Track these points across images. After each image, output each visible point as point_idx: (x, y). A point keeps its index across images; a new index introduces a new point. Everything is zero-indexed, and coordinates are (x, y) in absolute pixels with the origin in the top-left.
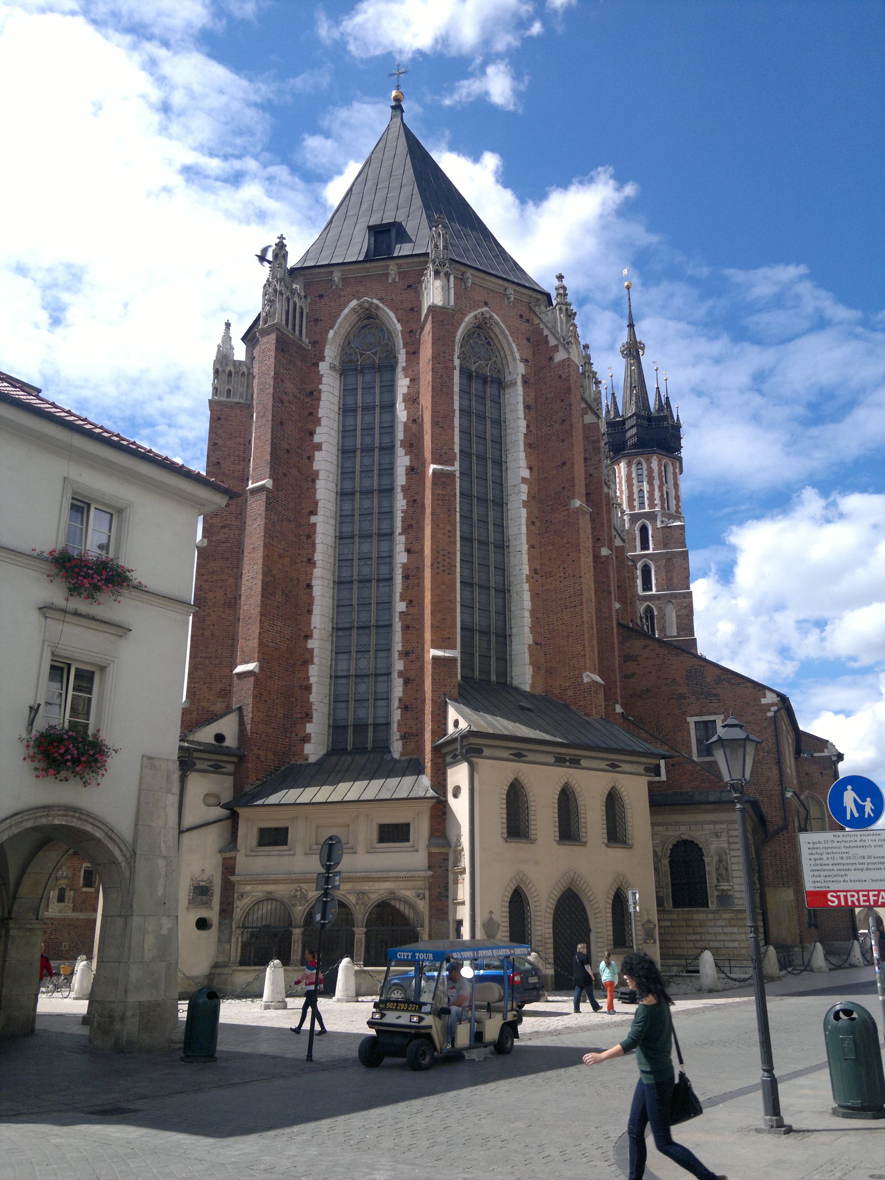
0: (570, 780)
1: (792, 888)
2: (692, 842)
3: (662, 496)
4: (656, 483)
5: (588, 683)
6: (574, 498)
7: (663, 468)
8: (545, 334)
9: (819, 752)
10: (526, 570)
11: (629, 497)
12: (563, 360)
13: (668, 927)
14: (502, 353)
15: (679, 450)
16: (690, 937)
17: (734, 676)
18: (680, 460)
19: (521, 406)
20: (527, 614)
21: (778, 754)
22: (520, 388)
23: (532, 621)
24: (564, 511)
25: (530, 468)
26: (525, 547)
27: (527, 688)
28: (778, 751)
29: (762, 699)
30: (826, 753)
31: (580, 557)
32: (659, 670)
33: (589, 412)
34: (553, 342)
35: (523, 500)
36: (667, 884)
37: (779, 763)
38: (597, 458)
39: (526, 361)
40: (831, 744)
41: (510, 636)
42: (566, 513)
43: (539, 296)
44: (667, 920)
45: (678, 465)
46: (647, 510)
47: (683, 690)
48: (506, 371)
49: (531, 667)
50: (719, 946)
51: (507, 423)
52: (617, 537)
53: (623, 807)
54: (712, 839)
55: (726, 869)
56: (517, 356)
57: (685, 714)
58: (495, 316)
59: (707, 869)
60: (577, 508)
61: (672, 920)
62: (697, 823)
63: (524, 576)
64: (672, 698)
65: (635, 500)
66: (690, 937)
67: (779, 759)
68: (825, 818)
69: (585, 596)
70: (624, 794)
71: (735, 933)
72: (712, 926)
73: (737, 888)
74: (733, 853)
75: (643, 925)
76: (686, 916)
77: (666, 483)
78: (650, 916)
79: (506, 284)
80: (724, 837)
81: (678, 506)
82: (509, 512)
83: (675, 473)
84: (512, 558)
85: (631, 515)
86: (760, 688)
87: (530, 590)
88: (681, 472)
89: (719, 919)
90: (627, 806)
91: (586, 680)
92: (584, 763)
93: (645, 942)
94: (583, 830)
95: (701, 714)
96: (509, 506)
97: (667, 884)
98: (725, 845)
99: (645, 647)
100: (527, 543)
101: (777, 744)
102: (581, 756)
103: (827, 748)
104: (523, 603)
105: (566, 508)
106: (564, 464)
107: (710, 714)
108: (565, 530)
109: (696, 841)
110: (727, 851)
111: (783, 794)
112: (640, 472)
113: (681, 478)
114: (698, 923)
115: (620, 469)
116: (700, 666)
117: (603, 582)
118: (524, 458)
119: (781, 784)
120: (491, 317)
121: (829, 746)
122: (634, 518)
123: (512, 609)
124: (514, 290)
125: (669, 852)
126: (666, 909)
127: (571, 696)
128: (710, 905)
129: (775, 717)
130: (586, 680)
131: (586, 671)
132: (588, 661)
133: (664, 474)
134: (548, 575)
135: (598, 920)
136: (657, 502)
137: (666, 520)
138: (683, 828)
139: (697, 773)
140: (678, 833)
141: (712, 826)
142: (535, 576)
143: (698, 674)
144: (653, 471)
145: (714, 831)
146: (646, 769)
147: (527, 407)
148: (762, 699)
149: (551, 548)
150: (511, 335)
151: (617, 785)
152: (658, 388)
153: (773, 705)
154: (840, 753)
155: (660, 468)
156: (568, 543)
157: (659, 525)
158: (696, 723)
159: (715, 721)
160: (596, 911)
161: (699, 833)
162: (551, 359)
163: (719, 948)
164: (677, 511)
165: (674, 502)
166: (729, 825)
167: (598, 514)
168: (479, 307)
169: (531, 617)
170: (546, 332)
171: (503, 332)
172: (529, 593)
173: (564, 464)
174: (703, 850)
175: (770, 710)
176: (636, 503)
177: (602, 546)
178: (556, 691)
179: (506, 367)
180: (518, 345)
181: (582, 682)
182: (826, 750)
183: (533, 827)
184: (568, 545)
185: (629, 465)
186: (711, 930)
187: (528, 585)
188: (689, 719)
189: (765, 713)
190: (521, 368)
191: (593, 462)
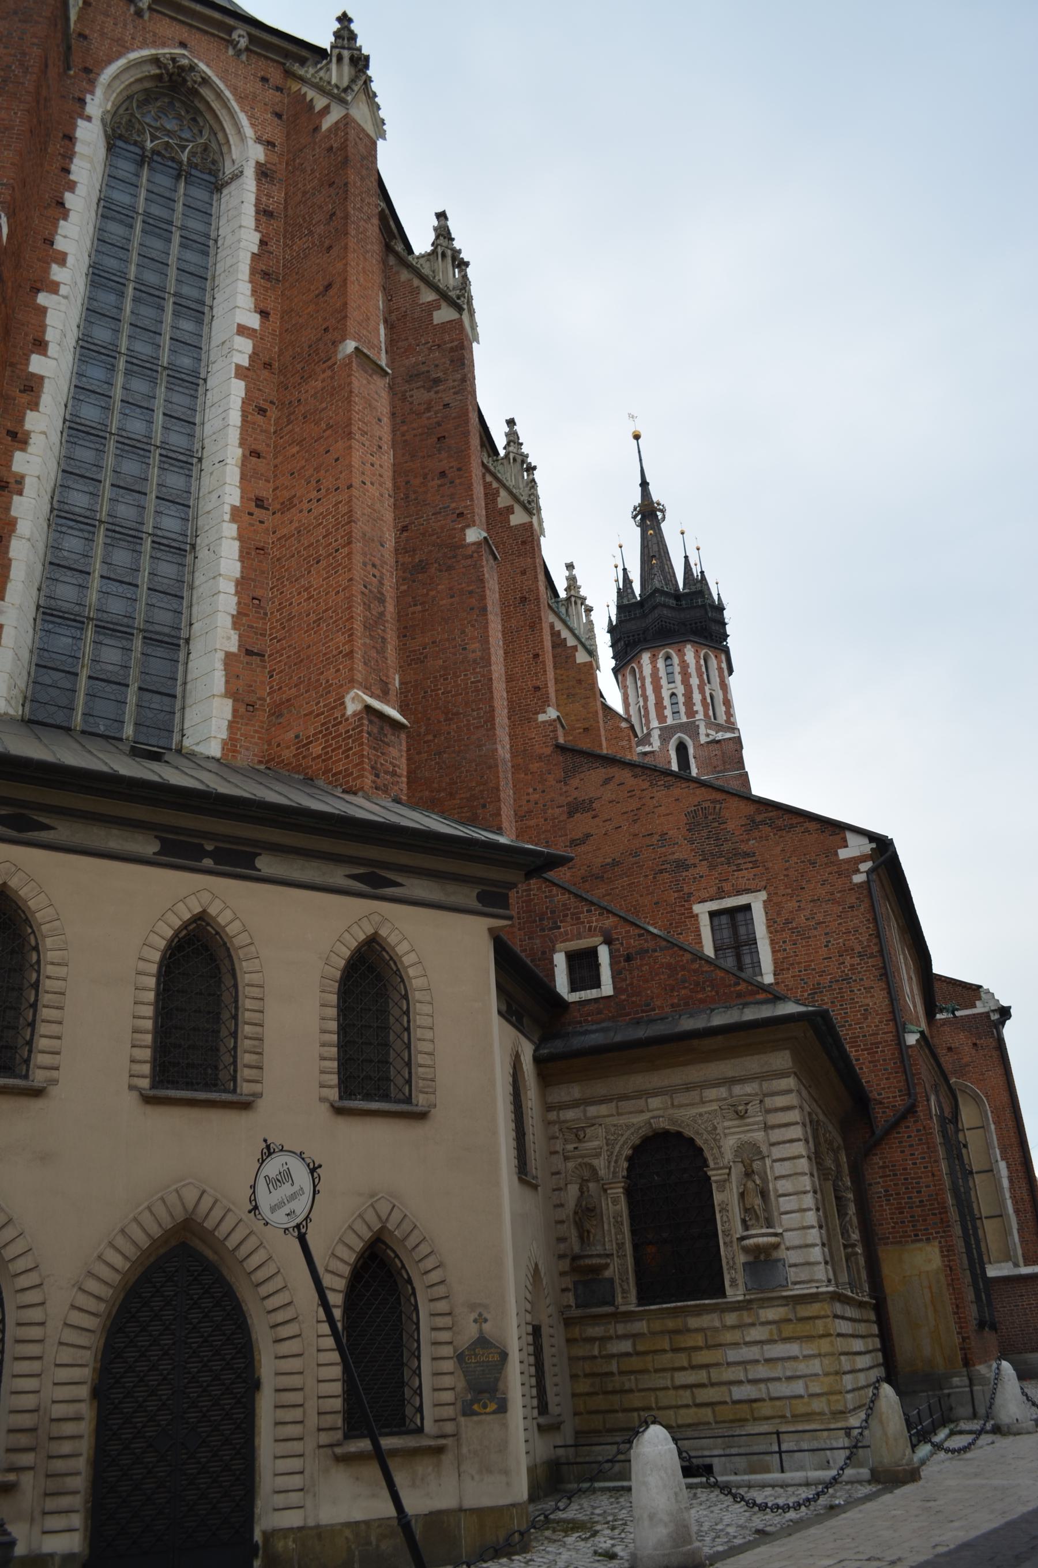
0: (212, 911)
1: (936, 1243)
2: (679, 1135)
3: (704, 699)
4: (694, 681)
5: (355, 714)
6: (344, 340)
7: (702, 662)
8: (308, 99)
9: (966, 1008)
10: (233, 496)
11: (656, 704)
12: (337, 123)
13: (627, 1354)
14: (220, 136)
15: (725, 640)
16: (682, 1378)
17: (780, 813)
18: (727, 651)
19: (249, 211)
20: (228, 587)
21: (882, 956)
22: (249, 183)
23: (239, 603)
24: (324, 371)
25: (264, 314)
26: (234, 453)
27: (215, 750)
28: (881, 951)
29: (839, 851)
30: (980, 1008)
31: (350, 447)
32: (635, 821)
33: (444, 305)
34: (320, 102)
35: (238, 367)
36: (621, 1246)
37: (885, 974)
38: (459, 376)
39: (269, 144)
40: (988, 992)
41: (187, 641)
42: (329, 373)
43: (304, 53)
44: (625, 1337)
45: (723, 657)
46: (684, 719)
47: (682, 852)
48: (228, 163)
49: (228, 704)
50: (754, 1396)
51: (220, 243)
52: (580, 647)
53: (406, 997)
54: (727, 1124)
55: (764, 1194)
56: (249, 131)
57: (688, 899)
58: (202, 66)
59: (718, 1197)
60: (350, 356)
61: (635, 1336)
62: (688, 1088)
63: (227, 508)
64: (661, 871)
65: (665, 708)
66: (682, 1378)
67: (884, 968)
68: (988, 1124)
69: (360, 527)
70: (407, 960)
71: (795, 1358)
72: (736, 1345)
73: (792, 1238)
74: (777, 1152)
75: (460, 1358)
76: (671, 1324)
77: (709, 682)
78: (486, 1327)
79: (231, 22)
80: (757, 1118)
81: (729, 714)
82: (209, 393)
83: (720, 669)
84: (206, 480)
85: (661, 729)
86: (837, 829)
87: (240, 538)
88: (731, 671)
89: (753, 1325)
90: (418, 995)
91: (352, 708)
92: (266, 864)
93: (468, 1412)
94: (248, 1058)
95: (720, 895)
96: (210, 383)
97: (621, 1246)
98: (759, 1136)
99: (607, 781)
100: (242, 444)
101: (878, 936)
102: (255, 843)
103: (980, 999)
104: (219, 565)
105: (329, 363)
106: (328, 287)
107: (739, 893)
108: (324, 405)
109: (688, 1132)
110: (764, 1149)
111: (900, 1041)
112: (670, 669)
113: (733, 681)
114: (699, 1340)
115: (641, 668)
116: (714, 801)
117: (471, 592)
118: (249, 292)
119: (895, 1020)
120: (192, 68)
121: (983, 995)
122: (666, 733)
123: (197, 583)
124: (249, 35)
125: (626, 1165)
126: (622, 1309)
127: (320, 756)
128: (729, 1291)
129: (868, 882)
130: (352, 708)
131: (353, 687)
132: (359, 666)
133: (704, 669)
134: (287, 505)
135: (285, 1348)
136: (698, 707)
137: (713, 733)
138: (655, 1102)
139: (683, 968)
140: (646, 1116)
141: (723, 1092)
142: (257, 512)
143: (710, 817)
144: (688, 666)
145: (730, 1101)
146: (481, 898)
147: (263, 213)
148: (839, 851)
149: (297, 448)
150: (236, 100)
151: (383, 932)
152: (686, 557)
153: (863, 859)
154: (1003, 1007)
155: (698, 662)
156: (329, 427)
157: (703, 739)
158: (712, 914)
159: (747, 908)
160: (280, 1317)
161: (694, 1111)
162: (317, 129)
163: (755, 1401)
164: (728, 721)
165: (723, 709)
166: (765, 1085)
167: (459, 469)
168: (164, 45)
169: (237, 593)
170: (311, 94)
171: (219, 95)
172: (237, 544)
173: (328, 287)
174: (707, 1154)
175: (857, 871)
176: (668, 712)
177: (468, 526)
178: (287, 754)
179: (226, 157)
180: (251, 118)
181: (343, 715)
182: (978, 1003)
183: (43, 1043)
184: (329, 432)
185: (653, 660)
186: (732, 1355)
187: (235, 526)
188: (697, 908)
189: (849, 877)
190: (257, 153)
191: (451, 384)
